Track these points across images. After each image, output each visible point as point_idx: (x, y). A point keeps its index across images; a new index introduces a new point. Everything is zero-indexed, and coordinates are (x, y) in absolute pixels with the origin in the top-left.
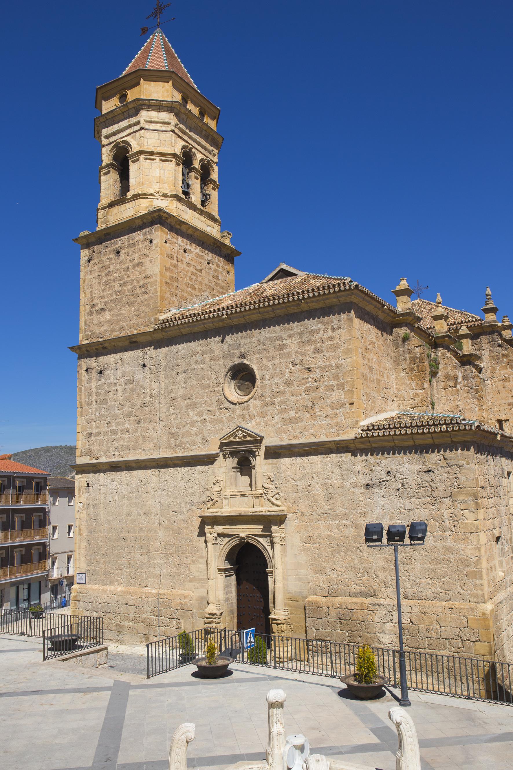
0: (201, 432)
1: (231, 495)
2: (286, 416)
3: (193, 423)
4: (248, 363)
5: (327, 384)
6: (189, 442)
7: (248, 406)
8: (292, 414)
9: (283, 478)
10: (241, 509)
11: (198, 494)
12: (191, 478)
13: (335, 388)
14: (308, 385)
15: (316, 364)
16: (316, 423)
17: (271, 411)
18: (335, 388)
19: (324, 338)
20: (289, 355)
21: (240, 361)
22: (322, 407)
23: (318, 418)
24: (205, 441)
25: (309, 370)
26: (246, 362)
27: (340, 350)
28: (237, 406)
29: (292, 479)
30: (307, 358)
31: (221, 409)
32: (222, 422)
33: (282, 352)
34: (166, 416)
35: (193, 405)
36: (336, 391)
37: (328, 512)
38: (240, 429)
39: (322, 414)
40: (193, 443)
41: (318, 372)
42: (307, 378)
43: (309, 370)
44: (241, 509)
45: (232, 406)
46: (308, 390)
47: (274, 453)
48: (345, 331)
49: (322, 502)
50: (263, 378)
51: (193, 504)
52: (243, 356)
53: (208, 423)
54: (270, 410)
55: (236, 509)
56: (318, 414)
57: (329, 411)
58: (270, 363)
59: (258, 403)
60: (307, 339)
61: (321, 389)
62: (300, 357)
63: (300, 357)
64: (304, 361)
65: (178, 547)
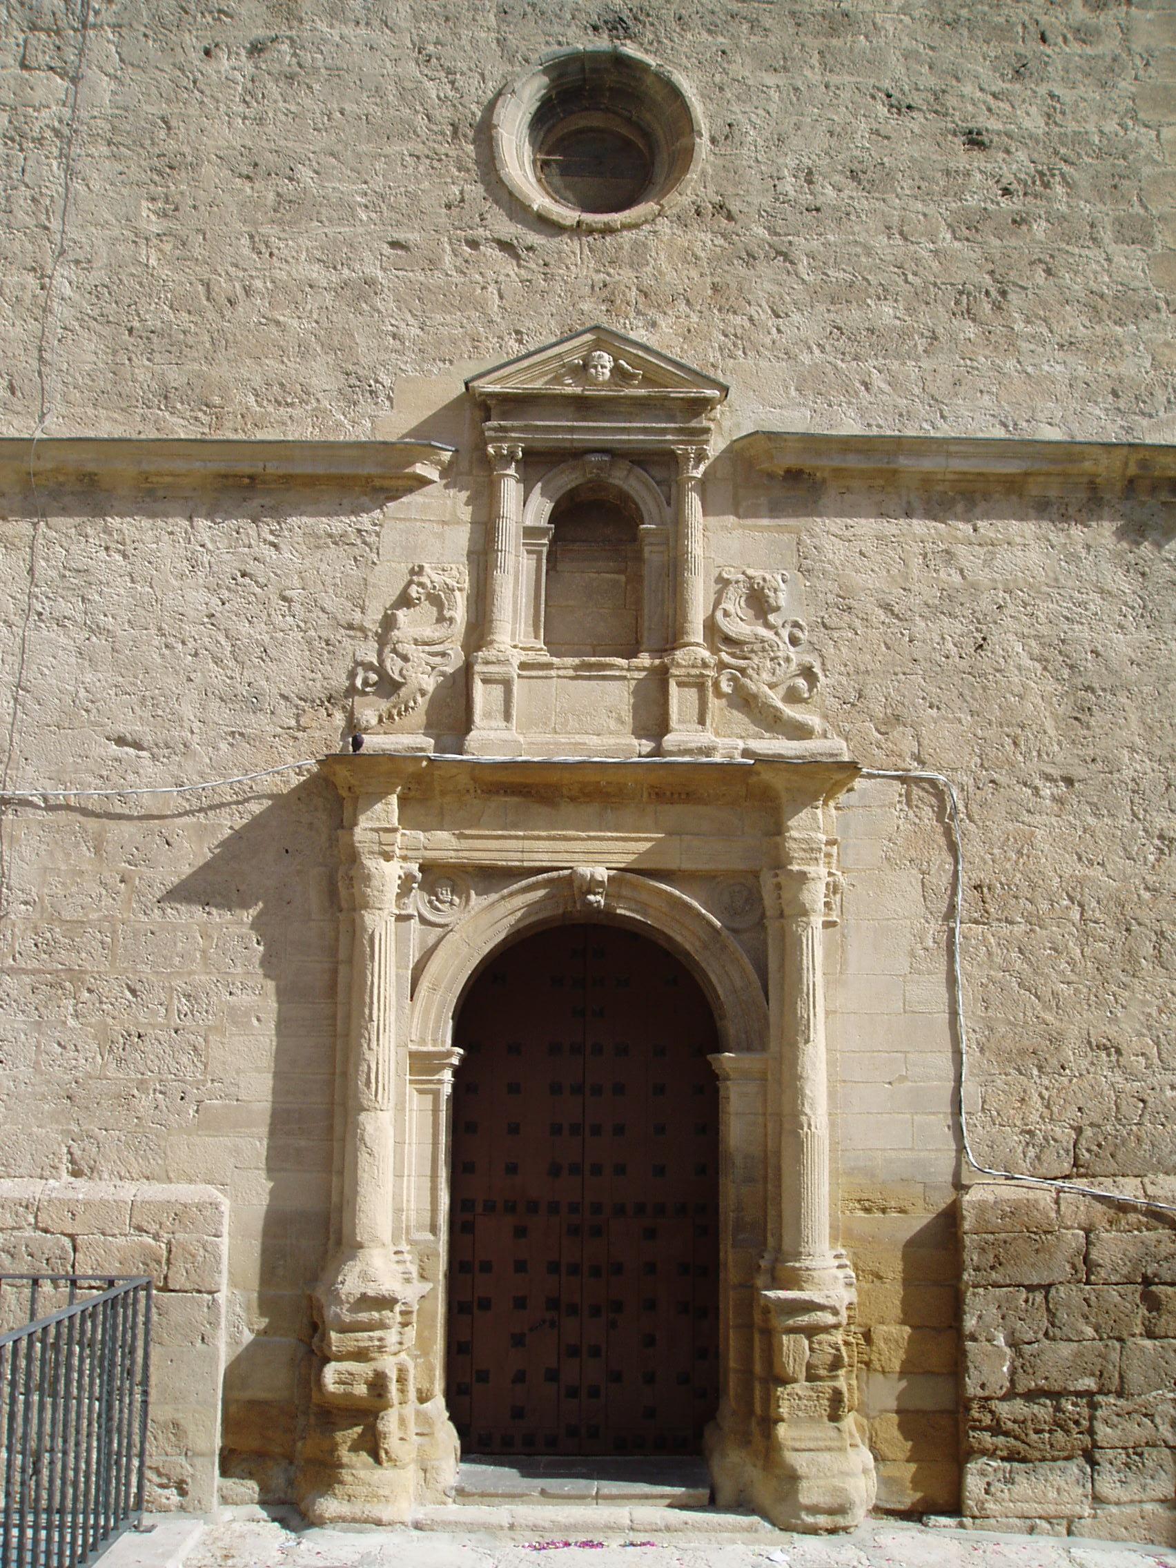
0: (338, 346)
1: (523, 666)
2: (853, 317)
3: (291, 294)
4: (651, 61)
5: (1064, 208)
6: (257, 381)
7: (639, 249)
8: (887, 313)
9: (831, 598)
10: (585, 739)
11: (295, 655)
12: (251, 567)
13: (1107, 236)
14: (972, 201)
15: (1011, 119)
16: (1010, 365)
17: (768, 286)
18: (1107, 236)
19: (1051, 25)
20: (875, 62)
21: (602, 43)
22: (1044, 304)
23: (1025, 346)
24: (358, 387)
25: (975, 140)
26: (630, 49)
27: (1125, 85)
28: (567, 244)
29: (888, 608)
30: (968, 89)
31: (474, 244)
32: (481, 307)
33: (834, 41)
34: (114, 241)
35: (292, 209)
36: (1112, 248)
37: (1079, 772)
38: (604, 338)
39: (1045, 331)
40: (285, 393)
41: (1022, 155)
42: (968, 174)
43: (975, 140)
44: (585, 739)
45: (534, 238)
46: (970, 225)
47: (789, 478)
48: (1150, 15)
49: (1049, 725)
50: (728, 134)
51: (254, 702)
52: (617, 25)
53: (385, 303)
54: (764, 281)
55: (548, 737)
56: (1019, 326)
57: (1076, 324)
58: (770, 79)
59: (703, 240)
60: (964, 12)
61: (1039, 229)
62: (929, 80)
63: (929, 80)
64: (951, 101)
65: (136, 934)
